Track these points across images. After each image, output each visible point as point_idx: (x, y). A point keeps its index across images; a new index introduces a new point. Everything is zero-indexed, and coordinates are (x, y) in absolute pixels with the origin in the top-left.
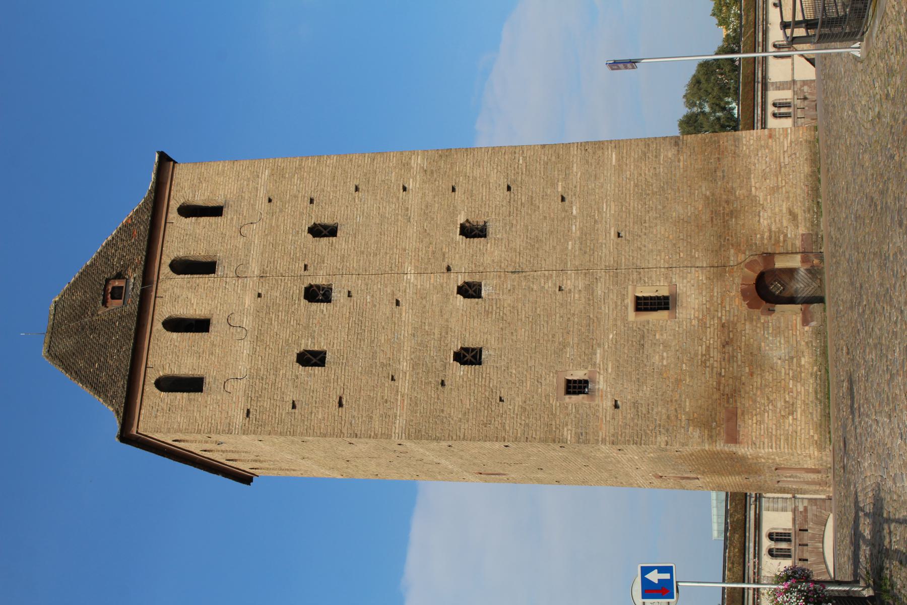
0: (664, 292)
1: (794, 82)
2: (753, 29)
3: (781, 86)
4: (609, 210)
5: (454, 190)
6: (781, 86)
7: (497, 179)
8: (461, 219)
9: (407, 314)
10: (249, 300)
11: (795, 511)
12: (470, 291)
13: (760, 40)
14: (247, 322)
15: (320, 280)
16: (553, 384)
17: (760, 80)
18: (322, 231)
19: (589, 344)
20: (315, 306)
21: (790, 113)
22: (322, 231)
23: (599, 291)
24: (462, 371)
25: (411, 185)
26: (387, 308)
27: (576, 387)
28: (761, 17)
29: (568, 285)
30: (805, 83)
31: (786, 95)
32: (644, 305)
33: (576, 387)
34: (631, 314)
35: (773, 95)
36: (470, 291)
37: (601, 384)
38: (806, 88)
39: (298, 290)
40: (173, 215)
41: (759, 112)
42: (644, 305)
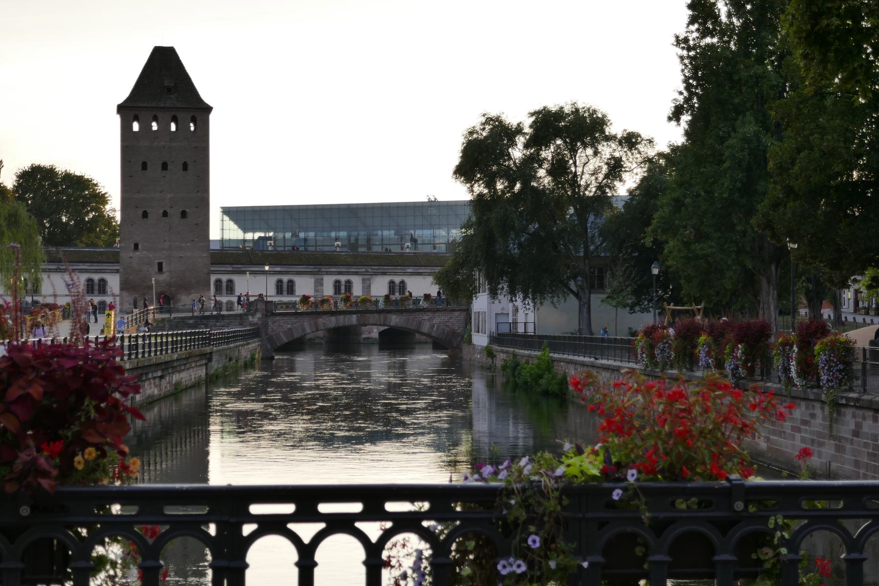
0: (164, 270)
5: (197, 207)
8: (187, 210)
10: (162, 143)
14: (156, 144)
15: (169, 167)
18: (185, 167)
20: (160, 166)
22: (185, 167)
23: (164, 252)
24: (140, 213)
25: (199, 194)
27: (136, 247)
29: (166, 243)
32: (160, 265)
33: (136, 247)
34: (157, 261)
36: (165, 214)
37: (137, 253)
40: (192, 114)
42: (160, 265)
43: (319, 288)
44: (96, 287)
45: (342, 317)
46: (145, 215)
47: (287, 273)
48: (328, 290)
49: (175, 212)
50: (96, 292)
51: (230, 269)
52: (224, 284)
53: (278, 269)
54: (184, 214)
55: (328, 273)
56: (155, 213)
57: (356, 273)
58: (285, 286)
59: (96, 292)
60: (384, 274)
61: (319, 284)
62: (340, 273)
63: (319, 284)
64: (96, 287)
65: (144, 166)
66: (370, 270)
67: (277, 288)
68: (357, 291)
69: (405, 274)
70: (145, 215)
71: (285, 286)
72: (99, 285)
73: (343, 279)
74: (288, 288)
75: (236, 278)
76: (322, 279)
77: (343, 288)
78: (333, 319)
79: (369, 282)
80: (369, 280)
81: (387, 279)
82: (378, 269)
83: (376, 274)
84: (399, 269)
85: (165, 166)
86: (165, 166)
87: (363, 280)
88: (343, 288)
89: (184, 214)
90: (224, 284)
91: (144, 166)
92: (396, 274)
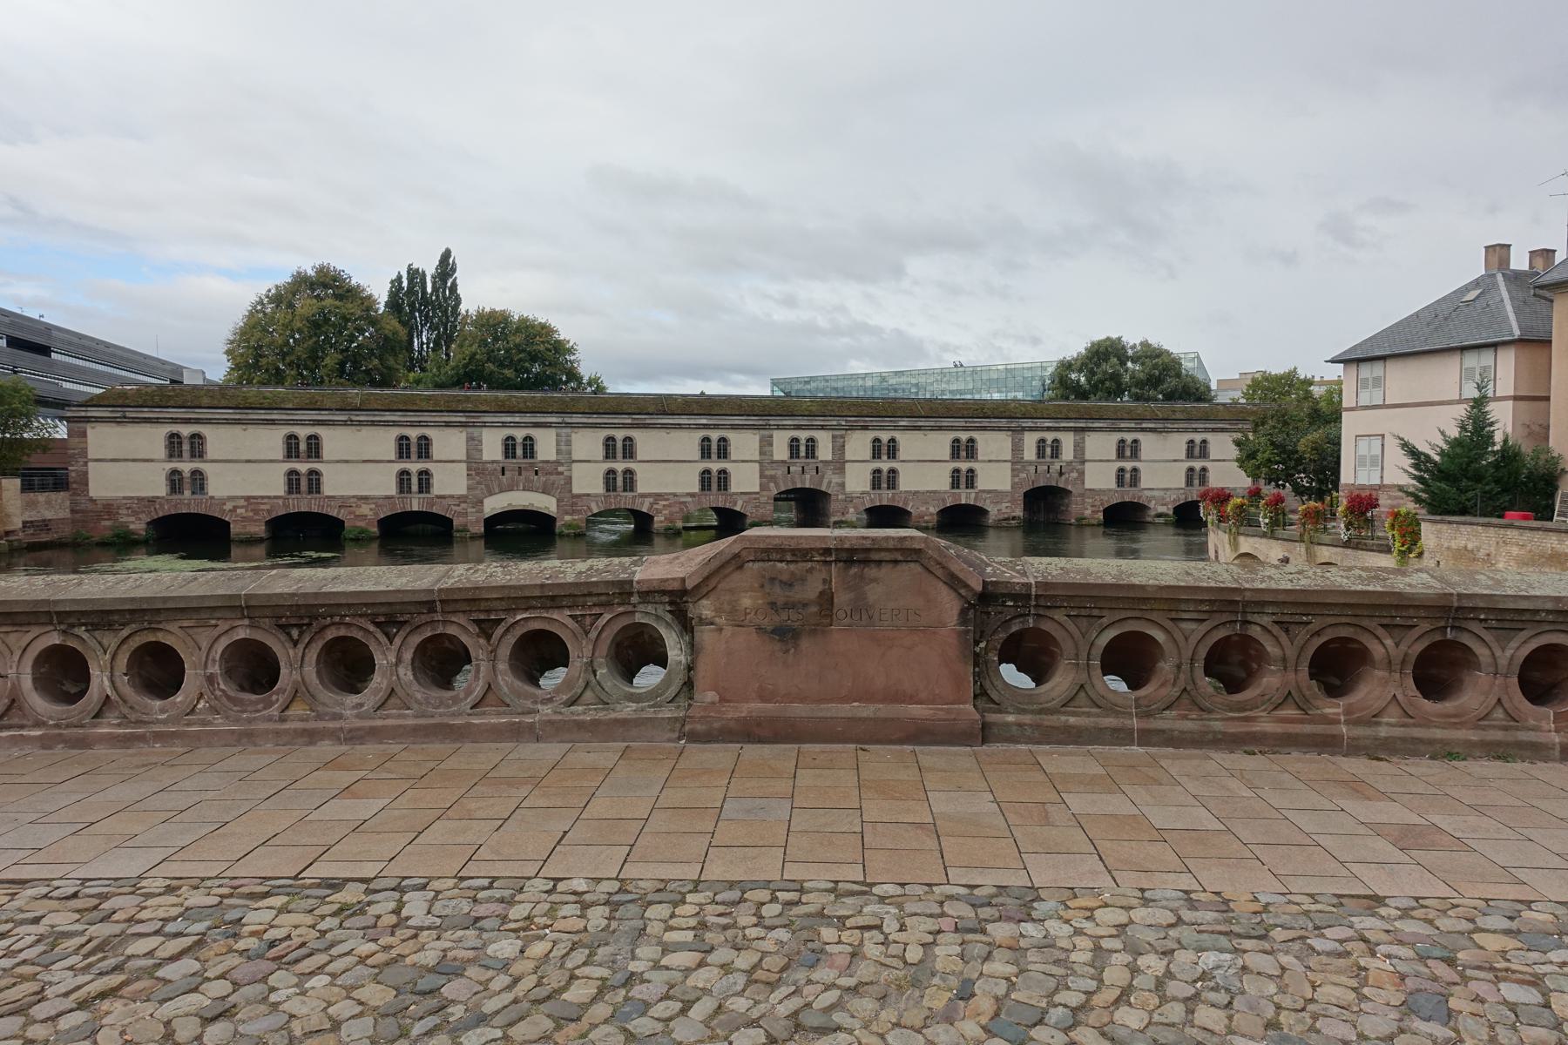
1: (1083, 462)
2: (1161, 416)
3: (1079, 448)
6: (1079, 448)
11: (558, 463)
13: (1144, 426)
17: (1091, 425)
21: (1043, 457)
28: (1176, 426)
30: (1082, 474)
31: (1067, 453)
35: (1068, 441)
38: (1075, 475)
41: (1047, 425)
43: (767, 449)
44: (414, 449)
47: (716, 427)
50: (414, 456)
51: (629, 421)
52: (619, 445)
53: (704, 421)
55: (779, 427)
57: (823, 428)
59: (414, 456)
60: (865, 428)
62: (798, 427)
63: (766, 443)
64: (414, 449)
66: (844, 423)
67: (703, 449)
69: (896, 428)
72: (420, 446)
73: (803, 435)
74: (719, 449)
75: (636, 434)
76: (771, 436)
77: (803, 449)
79: (842, 440)
80: (842, 437)
81: (871, 435)
82: (855, 421)
83: (852, 428)
84: (887, 422)
87: (833, 437)
88: (803, 449)
90: (619, 445)
92: (882, 428)
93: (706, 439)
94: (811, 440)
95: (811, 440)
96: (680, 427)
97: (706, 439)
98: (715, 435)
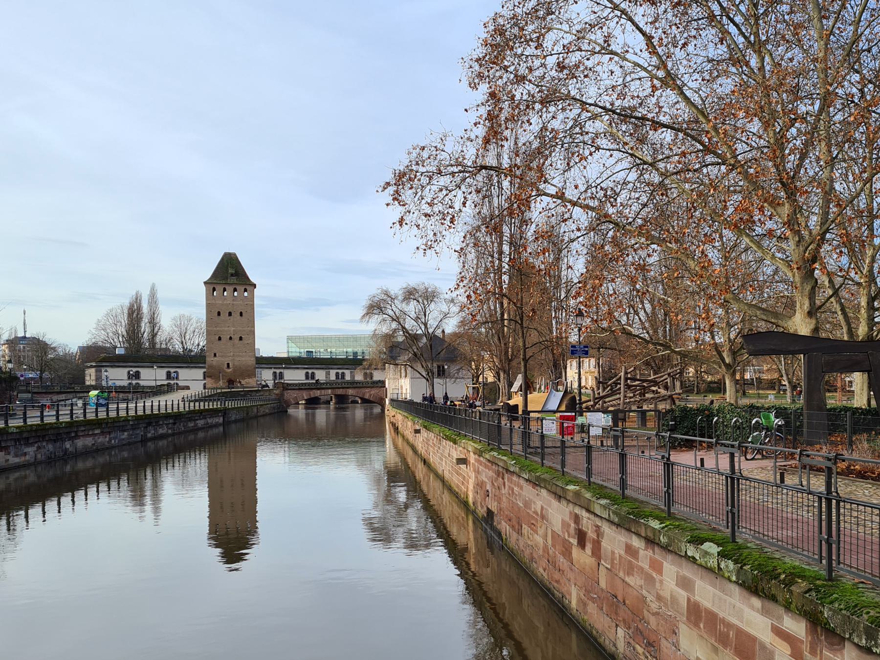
4: (243, 359)
7: (249, 342)
9: (226, 329)
12: (231, 338)
16: (216, 351)
18: (241, 314)
19: (222, 356)
22: (241, 314)
24: (217, 338)
26: (227, 325)
27: (215, 355)
32: (228, 364)
33: (215, 355)
36: (231, 338)
39: (231, 310)
42: (228, 364)
45: (323, 391)
46: (220, 339)
48: (333, 377)
49: (236, 338)
54: (241, 339)
55: (332, 369)
56: (225, 338)
57: (347, 369)
58: (310, 375)
61: (328, 374)
63: (328, 374)
65: (219, 314)
68: (348, 377)
70: (220, 339)
71: (310, 375)
73: (340, 371)
77: (340, 376)
78: (319, 391)
85: (230, 314)
86: (230, 314)
88: (340, 376)
89: (241, 339)
91: (219, 314)
93: (307, 373)
94: (343, 373)
95: (343, 373)
96: (298, 368)
97: (307, 373)
98: (310, 371)
